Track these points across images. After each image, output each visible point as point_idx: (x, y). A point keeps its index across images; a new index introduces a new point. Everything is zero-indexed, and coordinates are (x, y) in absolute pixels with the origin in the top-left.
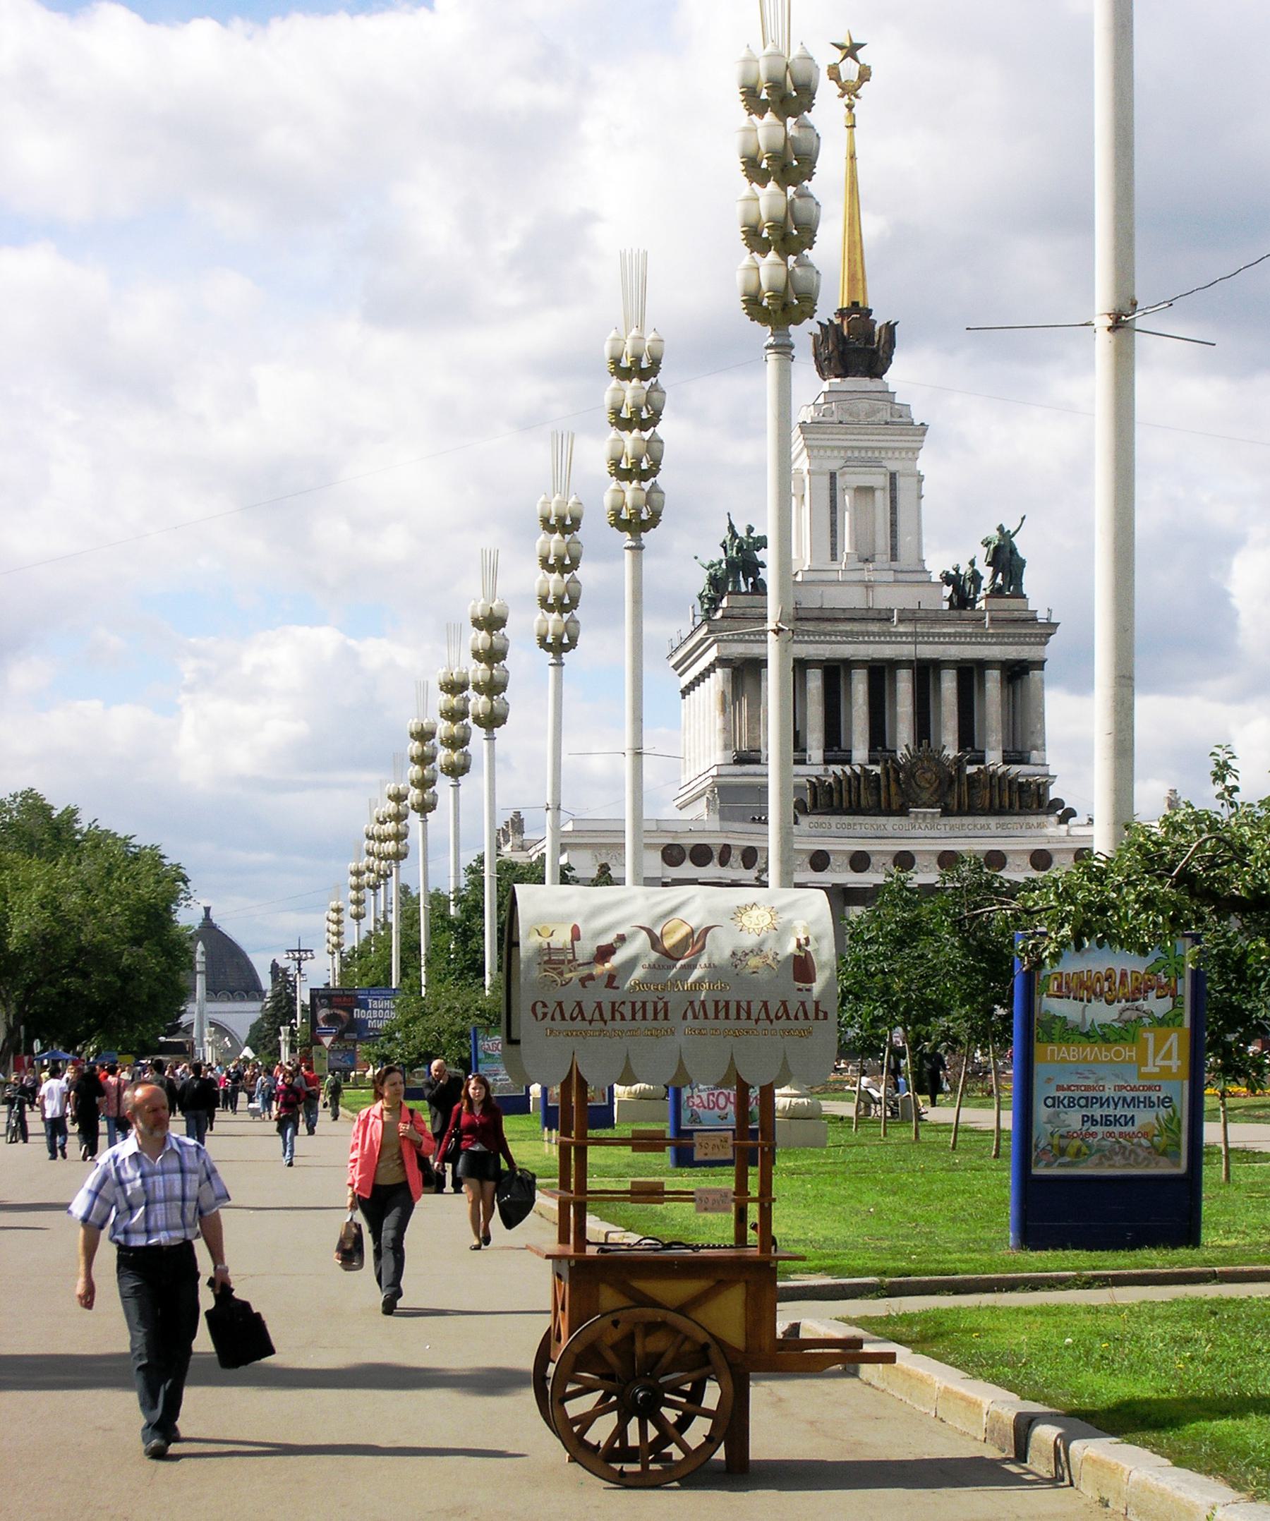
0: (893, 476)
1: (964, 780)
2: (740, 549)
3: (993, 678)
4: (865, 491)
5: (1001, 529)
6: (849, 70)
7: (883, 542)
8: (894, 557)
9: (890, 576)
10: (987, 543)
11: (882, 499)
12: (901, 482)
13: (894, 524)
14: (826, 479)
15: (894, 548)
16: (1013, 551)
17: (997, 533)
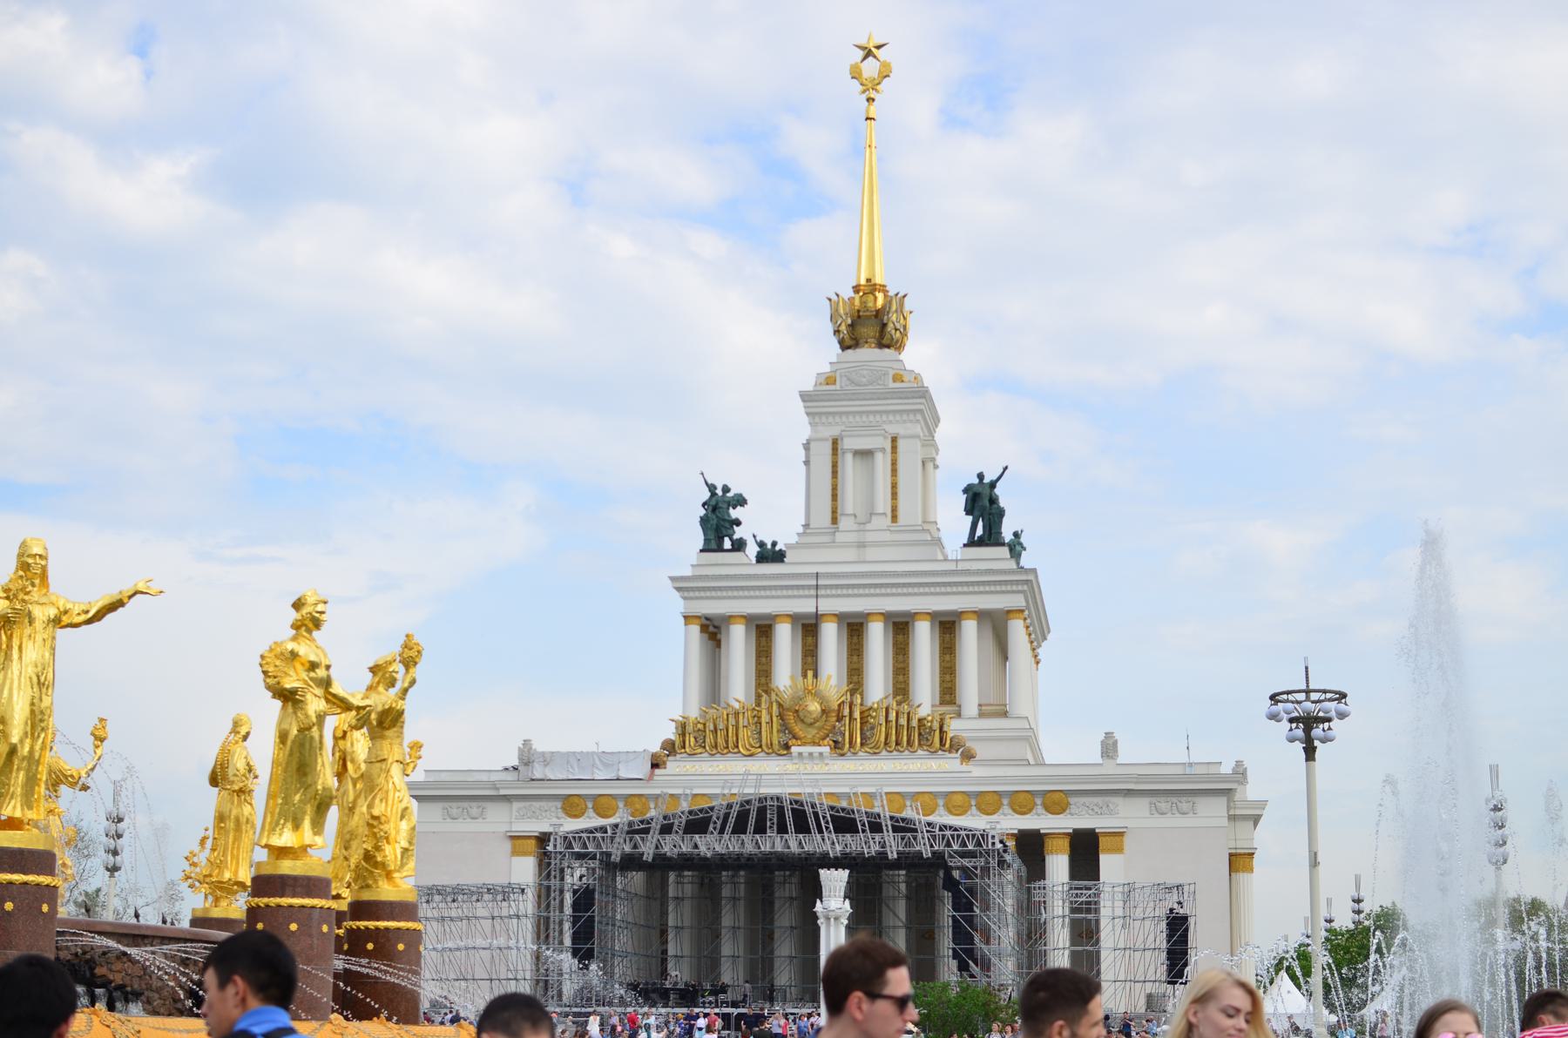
0: (894, 440)
1: (857, 715)
2: (715, 509)
3: (969, 629)
4: (865, 454)
5: (981, 476)
6: (870, 68)
7: (883, 503)
8: (894, 518)
9: (887, 536)
10: (966, 491)
11: (882, 463)
12: (901, 444)
13: (894, 486)
14: (829, 445)
15: (894, 510)
16: (993, 500)
17: (976, 481)
